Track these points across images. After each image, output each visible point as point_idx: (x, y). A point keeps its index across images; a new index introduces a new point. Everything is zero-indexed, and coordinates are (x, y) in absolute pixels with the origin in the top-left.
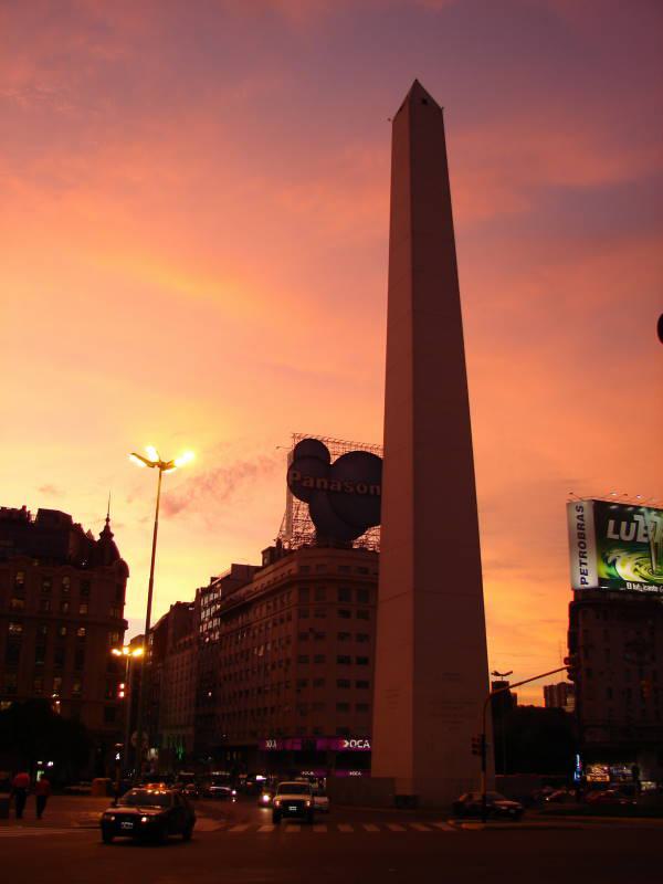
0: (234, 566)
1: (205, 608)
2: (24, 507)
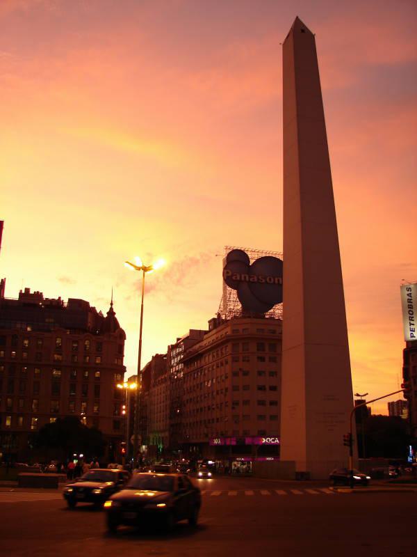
0: (191, 331)
1: (174, 358)
2: (60, 298)
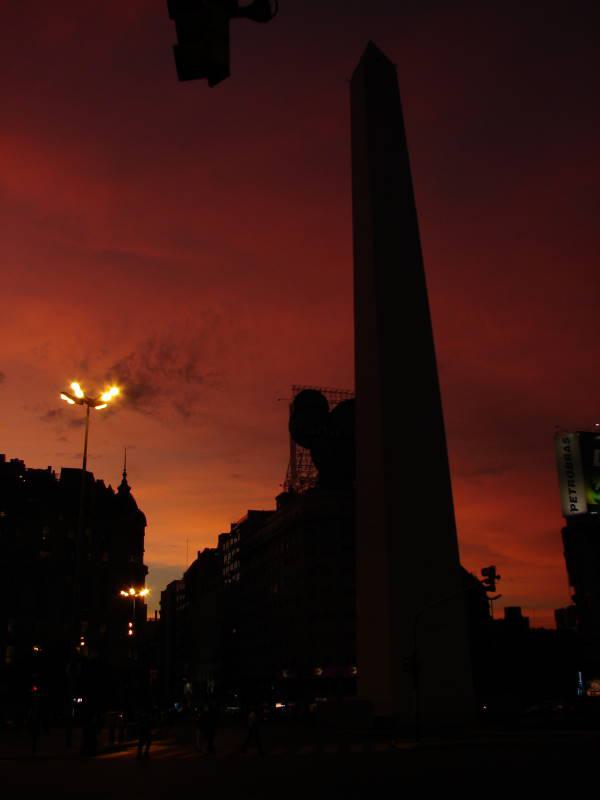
0: (250, 512)
